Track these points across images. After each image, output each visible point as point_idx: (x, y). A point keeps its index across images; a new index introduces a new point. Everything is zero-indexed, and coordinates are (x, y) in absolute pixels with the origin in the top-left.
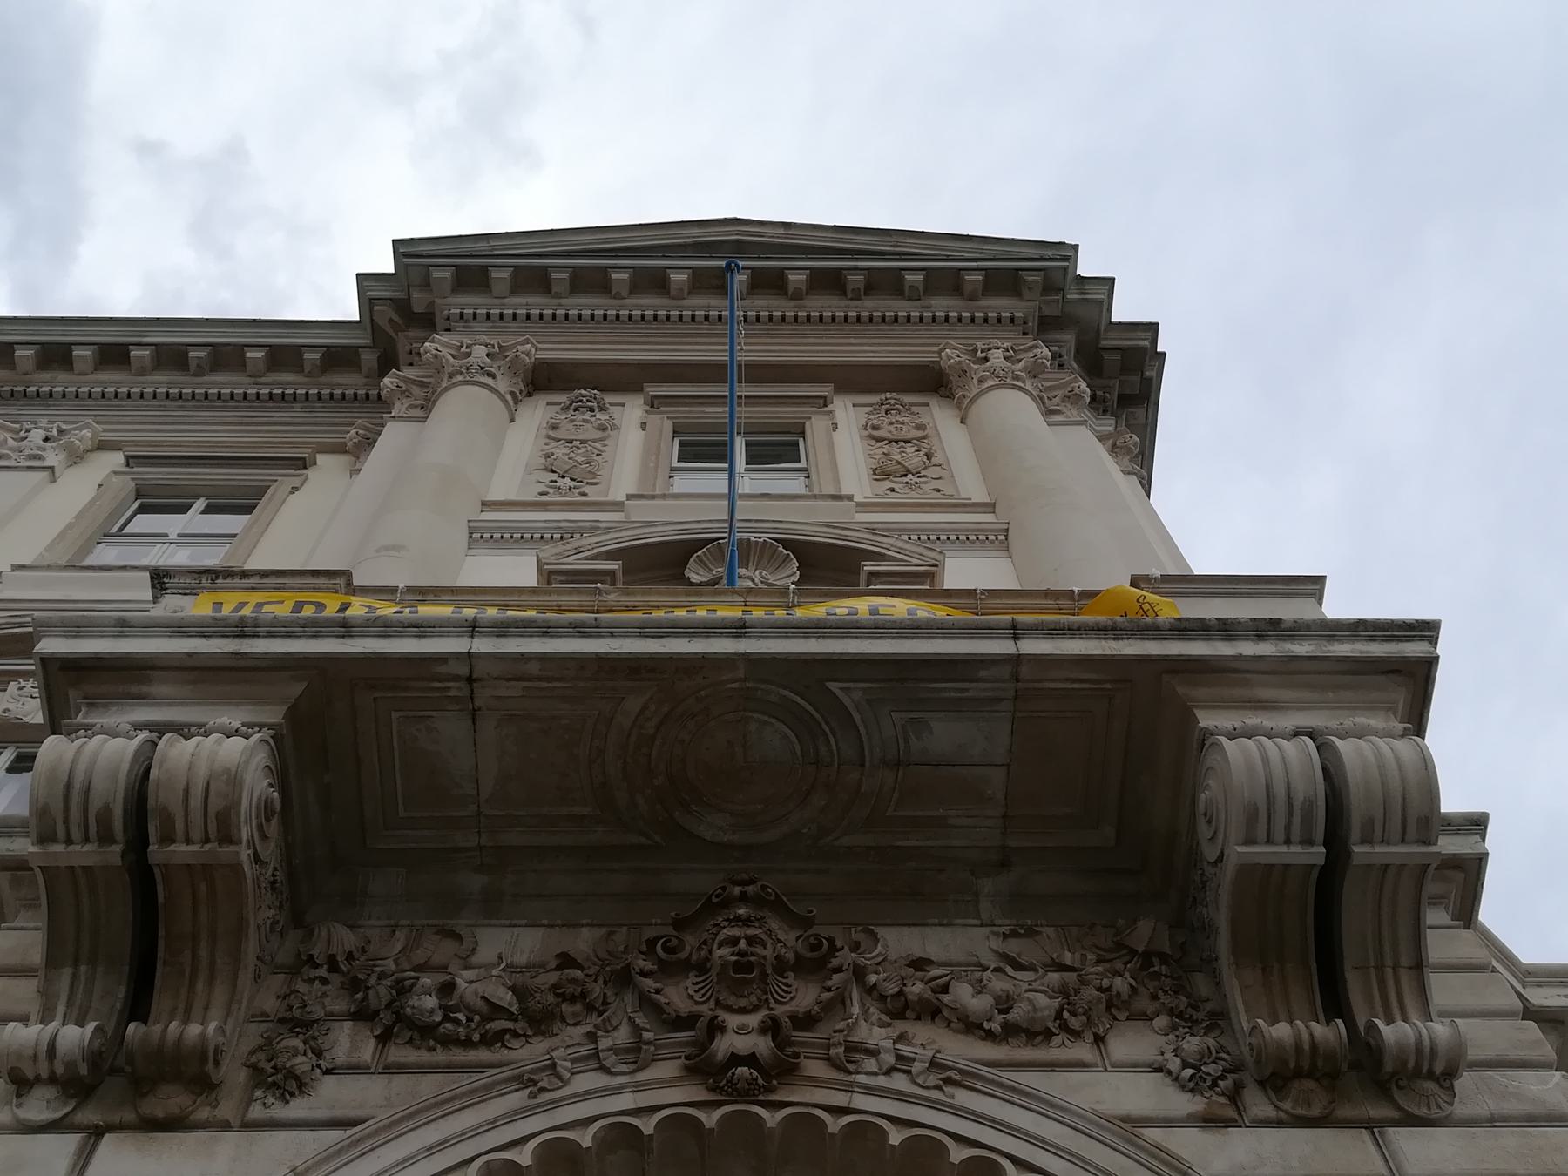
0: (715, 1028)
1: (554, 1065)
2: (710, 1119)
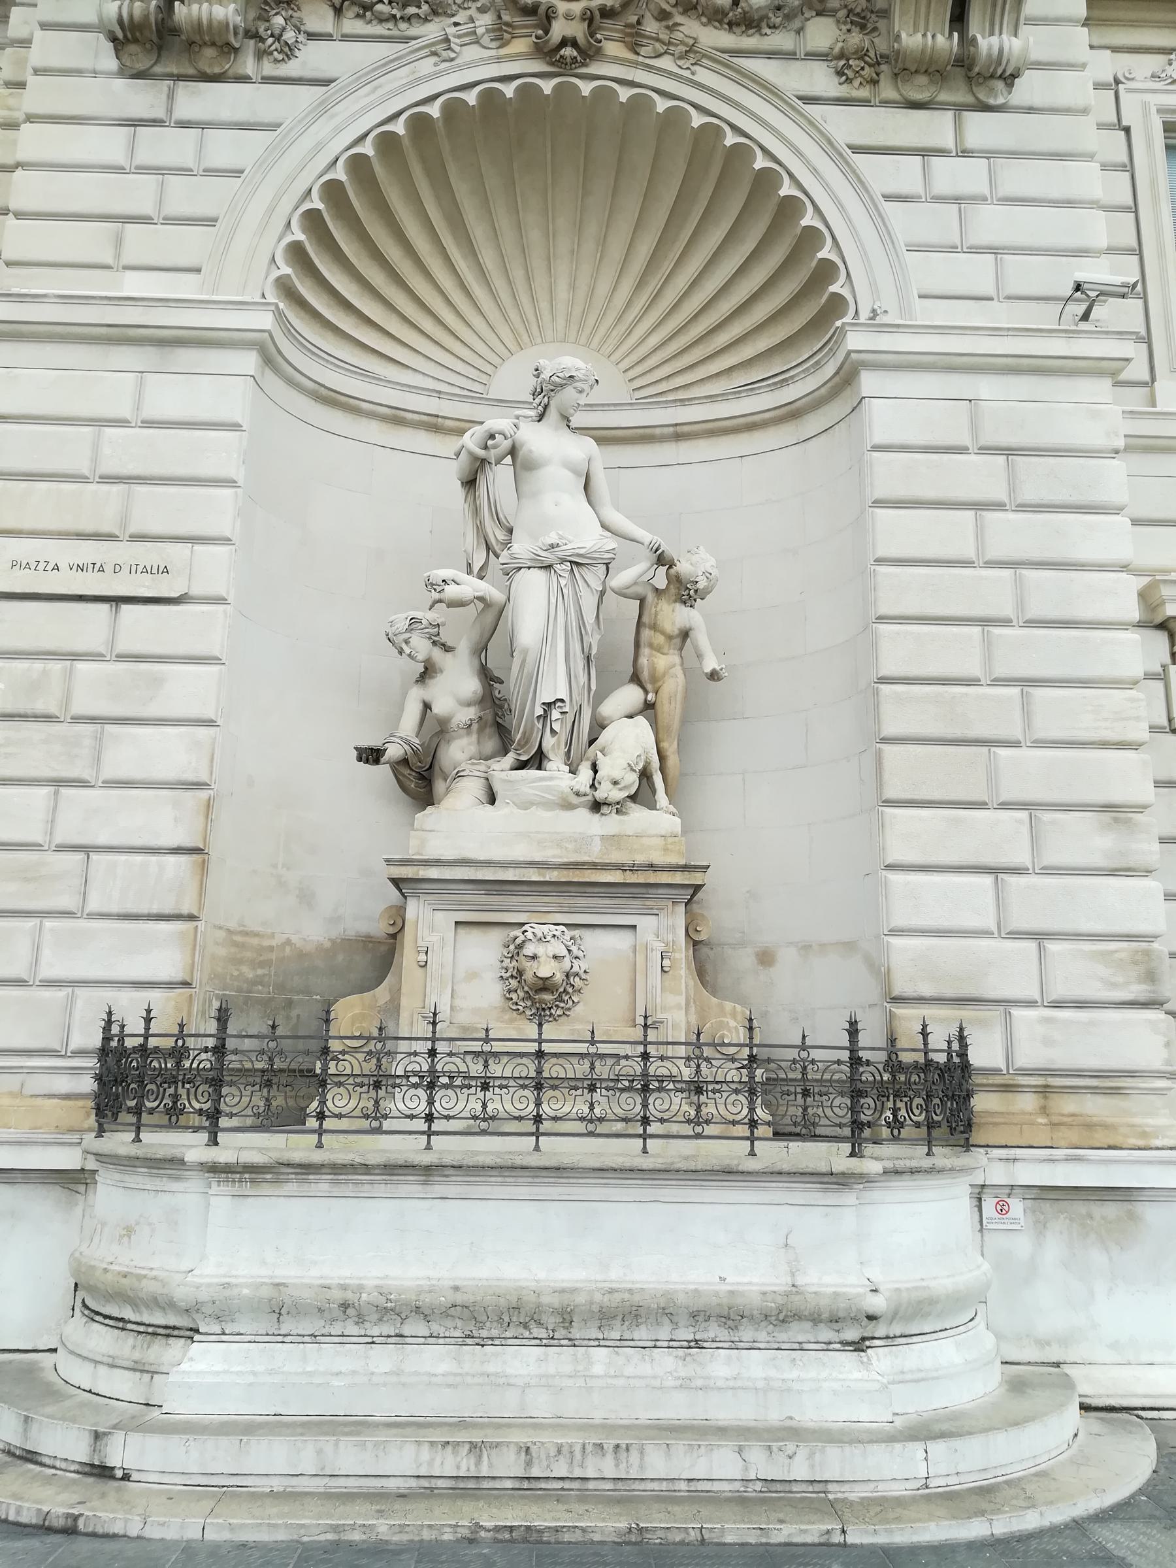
0: (549, 16)
1: (447, 40)
2: (547, 86)
